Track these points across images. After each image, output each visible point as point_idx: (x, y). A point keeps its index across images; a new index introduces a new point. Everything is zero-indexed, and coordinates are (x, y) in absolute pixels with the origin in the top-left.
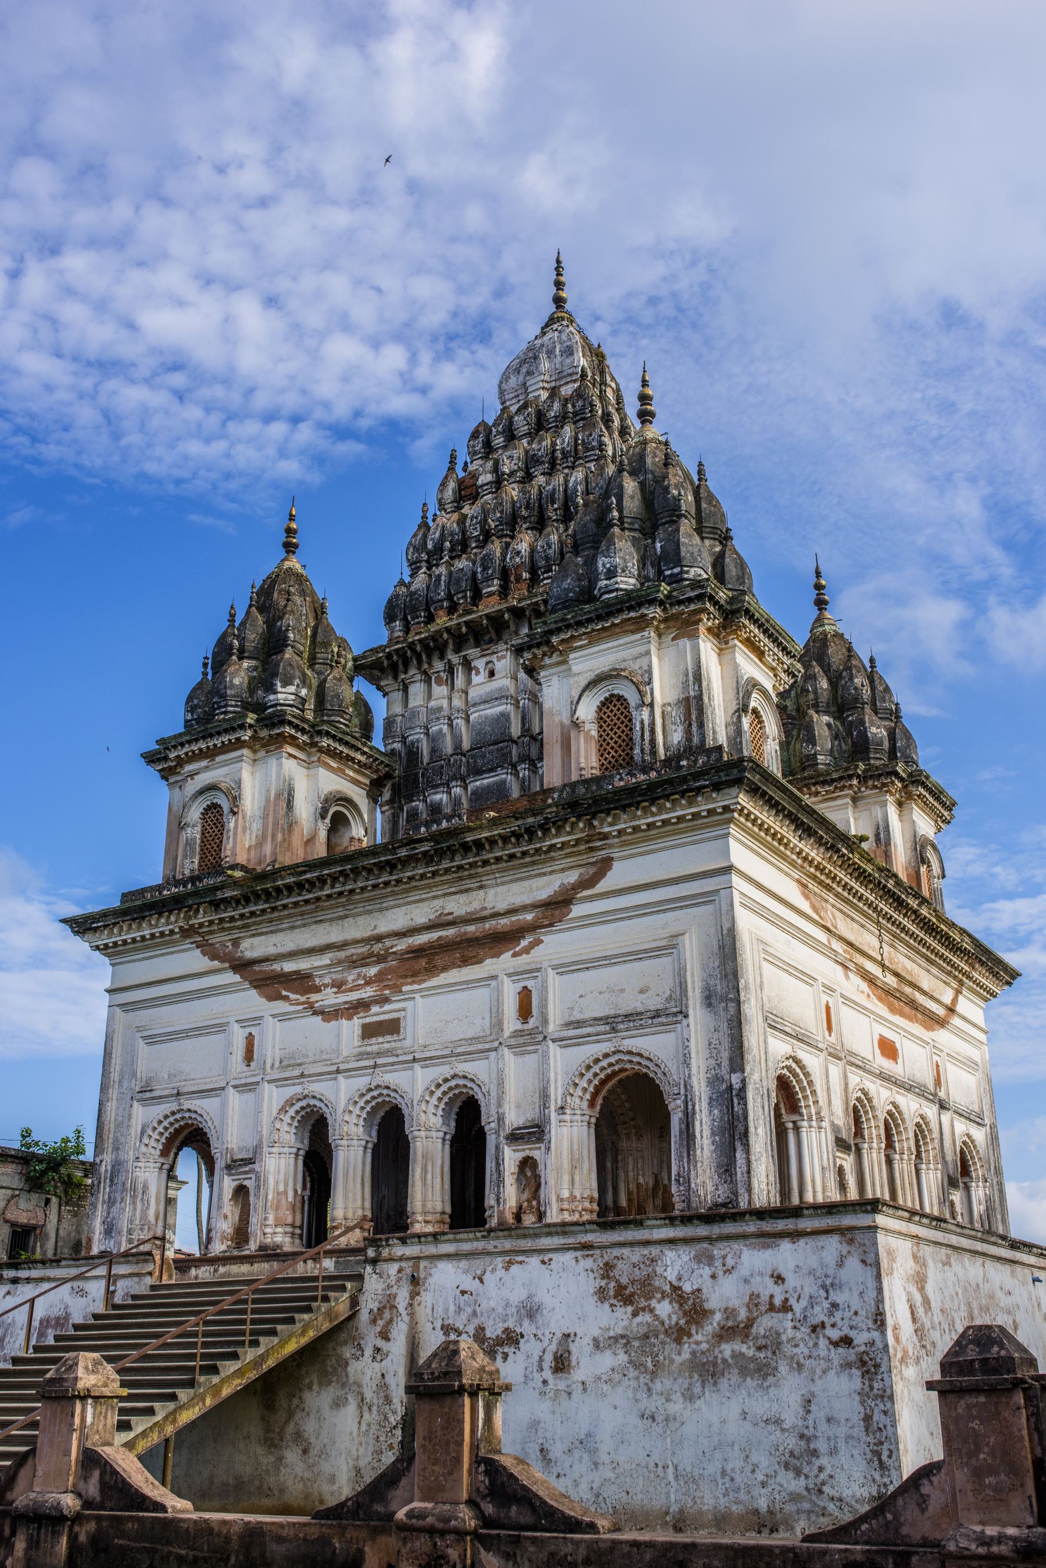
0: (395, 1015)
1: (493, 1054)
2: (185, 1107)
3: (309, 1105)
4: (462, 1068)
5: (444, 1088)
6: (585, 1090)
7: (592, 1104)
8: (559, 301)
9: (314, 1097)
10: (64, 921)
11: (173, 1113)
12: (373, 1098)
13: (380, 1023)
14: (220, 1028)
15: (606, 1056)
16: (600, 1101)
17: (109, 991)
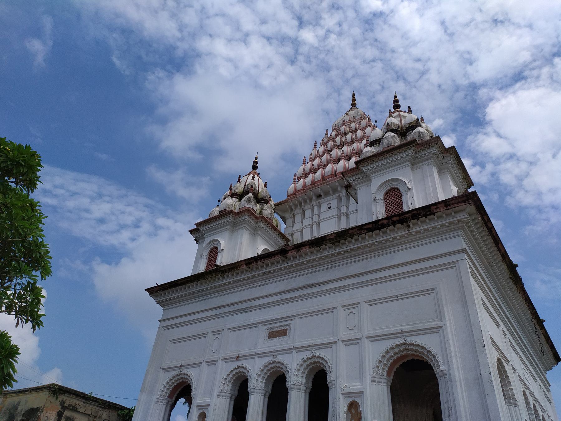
0: (285, 328)
1: (334, 345)
2: (182, 372)
3: (240, 372)
4: (317, 353)
5: (308, 363)
6: (385, 365)
7: (388, 374)
8: (354, 105)
9: (243, 367)
10: (147, 290)
11: (177, 375)
12: (272, 368)
13: (278, 331)
14: (204, 335)
15: (397, 346)
16: (393, 374)
17: (159, 321)
